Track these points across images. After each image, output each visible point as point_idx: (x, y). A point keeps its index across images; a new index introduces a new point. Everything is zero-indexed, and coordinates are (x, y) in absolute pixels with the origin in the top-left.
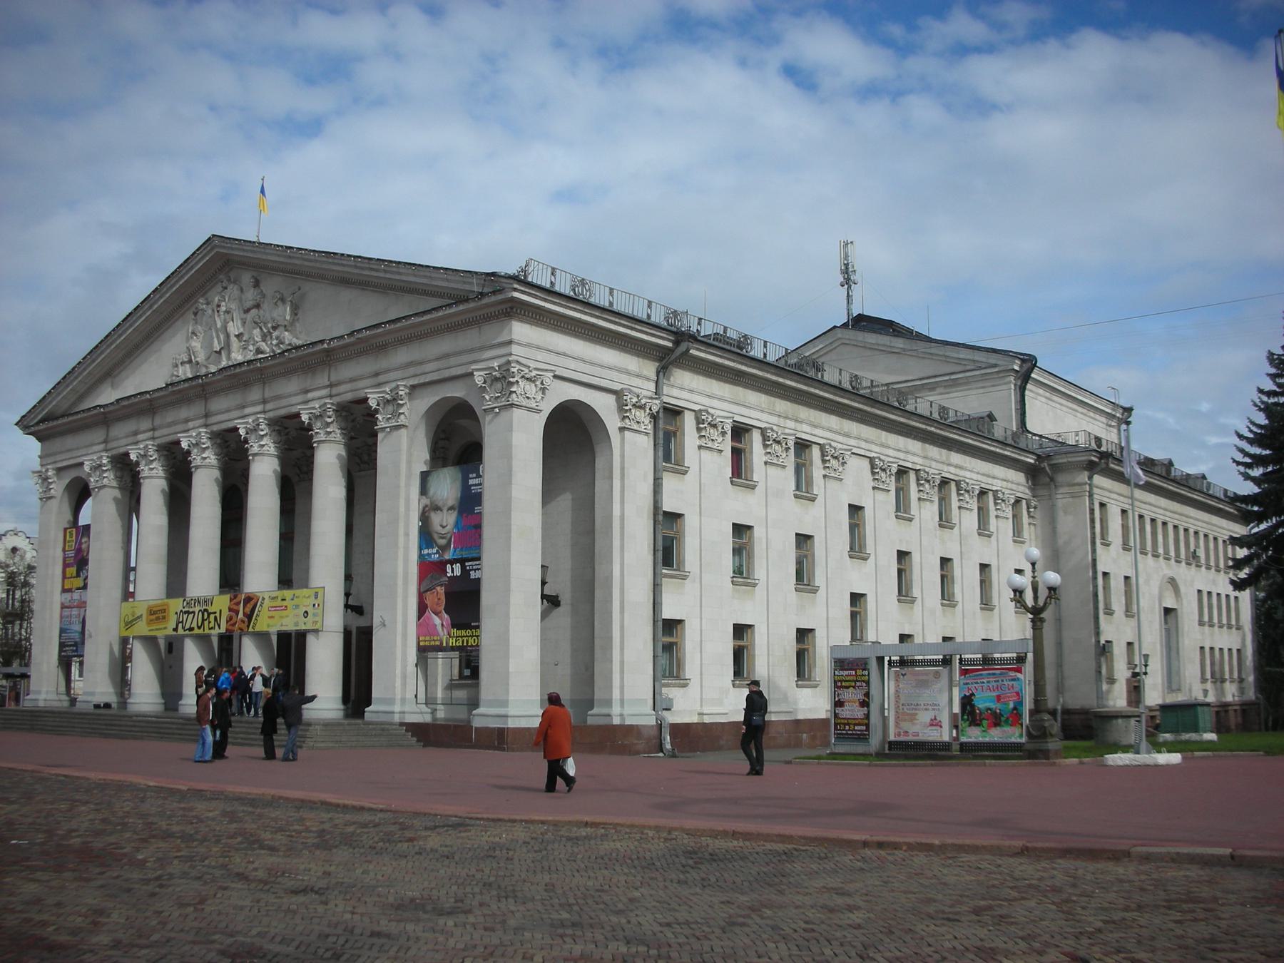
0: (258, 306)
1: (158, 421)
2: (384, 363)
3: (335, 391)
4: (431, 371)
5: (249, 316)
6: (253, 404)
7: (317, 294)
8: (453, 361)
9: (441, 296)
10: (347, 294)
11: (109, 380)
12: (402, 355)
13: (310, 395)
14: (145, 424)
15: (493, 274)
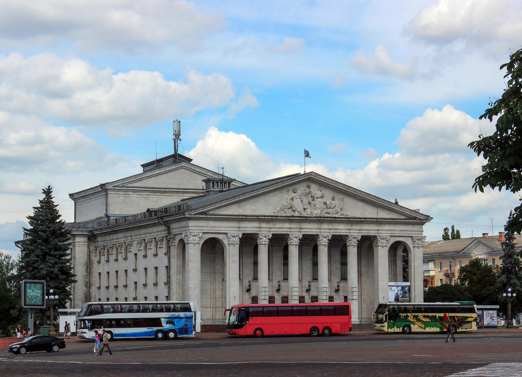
0: (322, 197)
1: (271, 225)
2: (380, 228)
3: (360, 231)
4: (397, 233)
5: (318, 200)
6: (325, 229)
7: (348, 201)
8: (404, 232)
9: (403, 215)
10: (360, 204)
11: (237, 204)
12: (387, 227)
13: (351, 231)
14: (264, 225)
15: (428, 216)
